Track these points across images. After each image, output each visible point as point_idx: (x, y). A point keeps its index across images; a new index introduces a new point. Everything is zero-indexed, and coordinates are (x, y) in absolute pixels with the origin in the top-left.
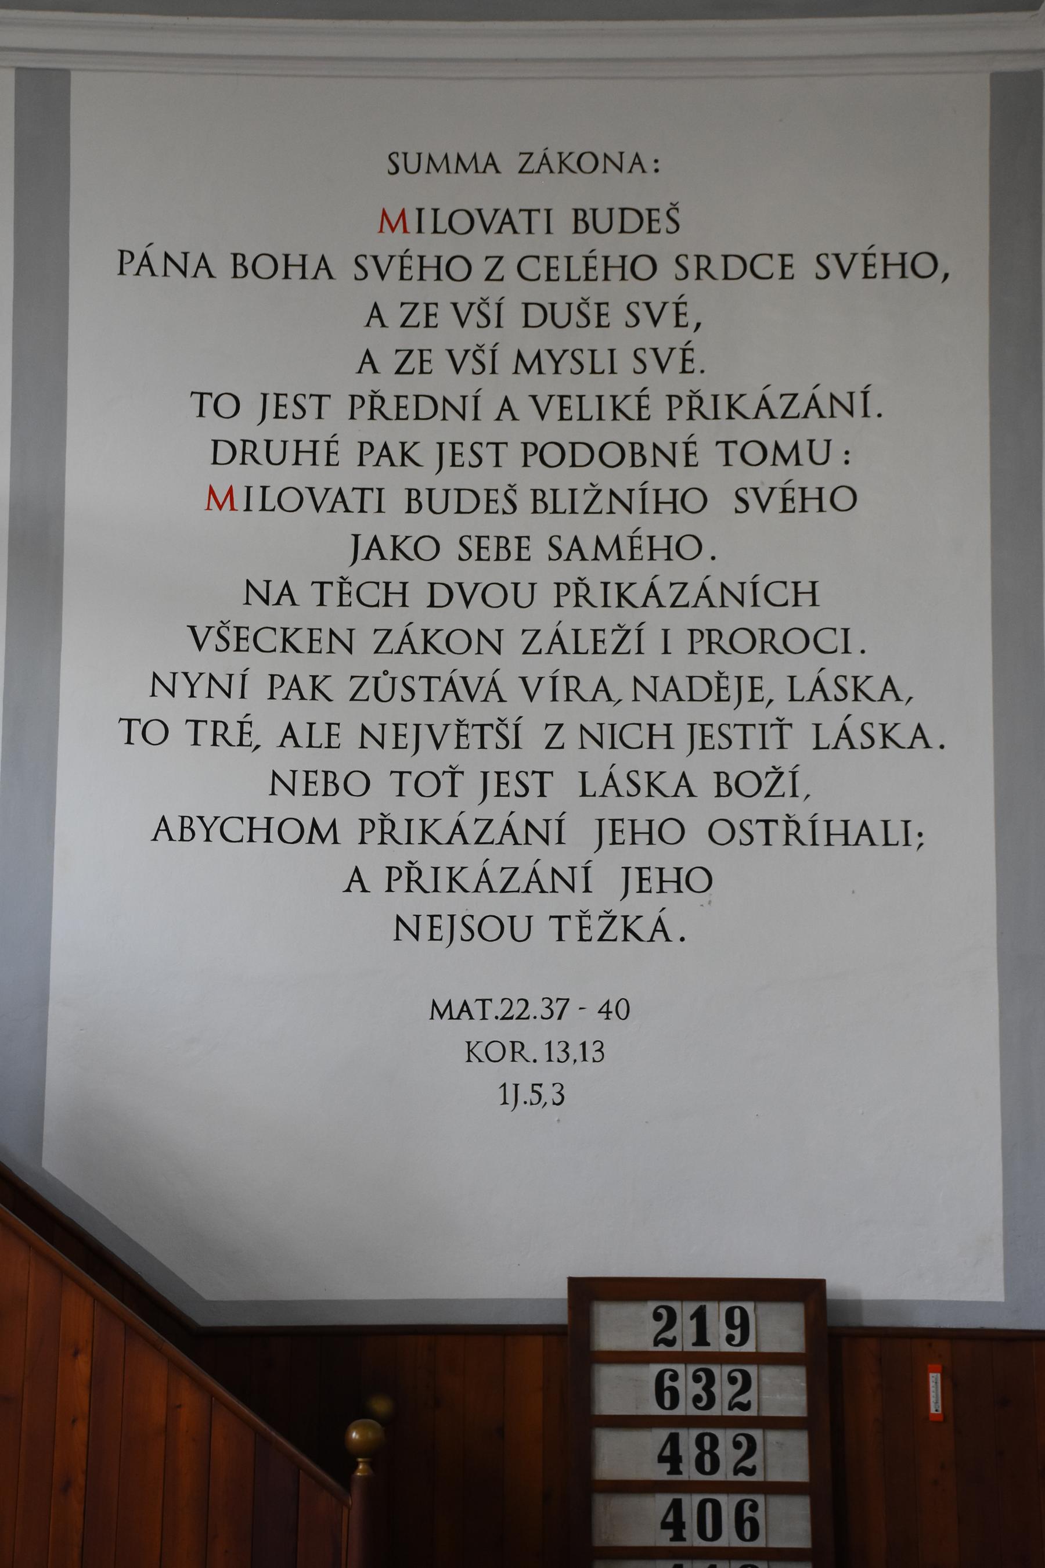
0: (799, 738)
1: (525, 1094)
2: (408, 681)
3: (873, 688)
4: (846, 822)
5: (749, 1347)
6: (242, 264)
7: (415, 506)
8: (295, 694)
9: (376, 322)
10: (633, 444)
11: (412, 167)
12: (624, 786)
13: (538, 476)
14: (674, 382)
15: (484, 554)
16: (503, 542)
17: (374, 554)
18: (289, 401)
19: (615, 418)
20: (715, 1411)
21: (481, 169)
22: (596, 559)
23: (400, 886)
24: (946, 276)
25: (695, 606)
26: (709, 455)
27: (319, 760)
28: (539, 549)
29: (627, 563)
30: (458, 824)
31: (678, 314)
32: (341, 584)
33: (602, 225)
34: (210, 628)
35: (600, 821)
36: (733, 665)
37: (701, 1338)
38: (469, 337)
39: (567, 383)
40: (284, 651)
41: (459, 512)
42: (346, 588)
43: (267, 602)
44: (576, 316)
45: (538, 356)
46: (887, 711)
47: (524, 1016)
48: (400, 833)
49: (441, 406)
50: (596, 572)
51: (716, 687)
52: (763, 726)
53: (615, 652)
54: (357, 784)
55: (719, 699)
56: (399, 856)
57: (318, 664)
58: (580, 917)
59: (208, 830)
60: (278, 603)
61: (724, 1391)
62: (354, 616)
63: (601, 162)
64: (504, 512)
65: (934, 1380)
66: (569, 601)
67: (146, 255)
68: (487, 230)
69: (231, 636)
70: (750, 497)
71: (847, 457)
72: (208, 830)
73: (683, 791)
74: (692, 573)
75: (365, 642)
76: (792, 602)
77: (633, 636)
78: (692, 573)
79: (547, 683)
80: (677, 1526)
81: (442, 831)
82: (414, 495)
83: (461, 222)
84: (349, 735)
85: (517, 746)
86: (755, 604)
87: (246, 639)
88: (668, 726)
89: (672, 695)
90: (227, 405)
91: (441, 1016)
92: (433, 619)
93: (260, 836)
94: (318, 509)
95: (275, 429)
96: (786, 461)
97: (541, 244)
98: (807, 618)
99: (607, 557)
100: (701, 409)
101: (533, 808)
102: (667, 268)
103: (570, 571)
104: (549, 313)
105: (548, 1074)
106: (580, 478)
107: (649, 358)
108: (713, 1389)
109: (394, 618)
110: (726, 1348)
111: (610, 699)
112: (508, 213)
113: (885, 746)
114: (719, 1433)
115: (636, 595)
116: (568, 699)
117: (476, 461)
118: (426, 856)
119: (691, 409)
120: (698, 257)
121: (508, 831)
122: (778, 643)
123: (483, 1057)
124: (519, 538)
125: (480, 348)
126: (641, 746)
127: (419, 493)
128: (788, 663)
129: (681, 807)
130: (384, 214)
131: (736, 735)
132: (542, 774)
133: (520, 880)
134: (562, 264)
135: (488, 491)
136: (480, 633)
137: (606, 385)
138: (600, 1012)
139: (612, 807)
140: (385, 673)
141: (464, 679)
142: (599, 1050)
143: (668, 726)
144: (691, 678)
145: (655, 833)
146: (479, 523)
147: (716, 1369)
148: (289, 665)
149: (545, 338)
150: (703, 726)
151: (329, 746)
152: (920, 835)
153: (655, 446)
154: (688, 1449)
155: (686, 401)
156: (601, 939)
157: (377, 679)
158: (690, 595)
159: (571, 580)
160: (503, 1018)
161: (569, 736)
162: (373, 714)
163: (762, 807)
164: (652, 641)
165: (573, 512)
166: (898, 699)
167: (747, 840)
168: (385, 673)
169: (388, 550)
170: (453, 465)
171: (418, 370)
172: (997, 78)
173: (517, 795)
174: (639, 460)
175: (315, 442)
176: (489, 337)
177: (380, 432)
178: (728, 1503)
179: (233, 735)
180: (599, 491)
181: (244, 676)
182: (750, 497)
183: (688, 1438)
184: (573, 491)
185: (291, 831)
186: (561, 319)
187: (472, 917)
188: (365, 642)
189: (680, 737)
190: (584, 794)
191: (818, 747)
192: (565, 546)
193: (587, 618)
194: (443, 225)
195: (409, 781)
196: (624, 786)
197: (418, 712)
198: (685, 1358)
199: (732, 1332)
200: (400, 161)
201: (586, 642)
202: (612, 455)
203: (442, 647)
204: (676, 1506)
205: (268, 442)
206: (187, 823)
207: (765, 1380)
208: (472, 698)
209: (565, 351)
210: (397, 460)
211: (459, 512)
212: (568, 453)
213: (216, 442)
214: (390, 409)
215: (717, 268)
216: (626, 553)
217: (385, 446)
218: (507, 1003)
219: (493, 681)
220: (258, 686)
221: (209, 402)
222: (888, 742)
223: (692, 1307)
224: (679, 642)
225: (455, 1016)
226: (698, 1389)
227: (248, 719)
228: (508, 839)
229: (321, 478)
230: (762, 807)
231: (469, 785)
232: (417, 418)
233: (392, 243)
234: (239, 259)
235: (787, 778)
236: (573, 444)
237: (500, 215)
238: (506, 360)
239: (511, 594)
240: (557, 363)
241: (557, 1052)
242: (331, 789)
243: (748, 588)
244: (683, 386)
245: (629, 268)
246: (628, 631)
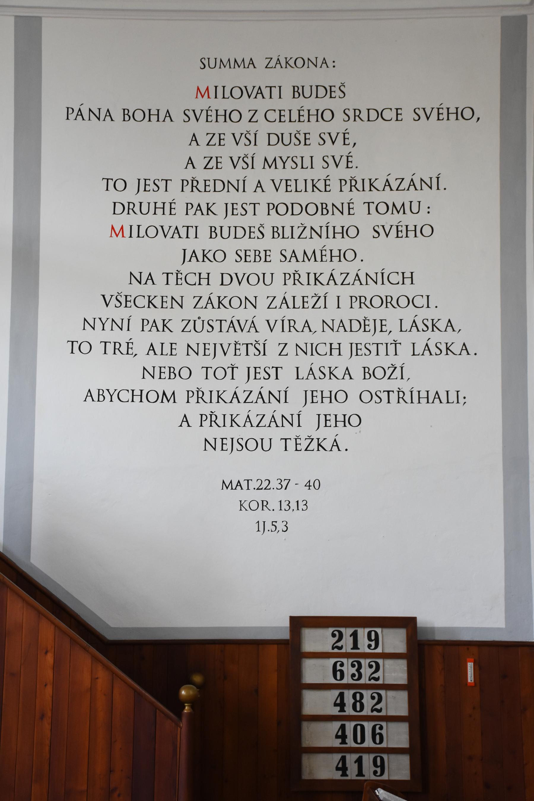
0: (405, 350)
1: (269, 526)
2: (210, 322)
3: (442, 325)
4: (428, 392)
5: (379, 650)
6: (127, 114)
7: (214, 235)
8: (154, 329)
9: (194, 143)
10: (322, 204)
11: (212, 65)
12: (318, 374)
13: (275, 220)
14: (343, 172)
15: (248, 259)
16: (257, 253)
17: (194, 259)
18: (151, 183)
19: (313, 191)
20: (362, 681)
21: (246, 66)
22: (304, 261)
23: (206, 423)
24: (478, 119)
25: (353, 284)
26: (360, 209)
27: (166, 361)
28: (275, 256)
29: (319, 263)
30: (235, 393)
31: (344, 139)
32: (177, 274)
33: (307, 94)
34: (112, 296)
35: (306, 391)
36: (372, 314)
37: (355, 646)
39: (289, 173)
40: (149, 307)
41: (235, 238)
42: (180, 276)
43: (140, 283)
44: (294, 140)
45: (275, 160)
46: (448, 337)
47: (268, 488)
48: (207, 398)
49: (227, 185)
50: (304, 268)
51: (363, 325)
52: (387, 344)
53: (313, 307)
54: (185, 373)
55: (365, 331)
56: (206, 409)
57: (166, 314)
58: (296, 439)
59: (111, 396)
60: (146, 283)
61: (366, 672)
62: (183, 290)
64: (258, 238)
65: (470, 666)
66: (290, 282)
67: (80, 110)
68: (249, 97)
69: (123, 300)
70: (381, 230)
71: (429, 210)
72: (111, 396)
73: (347, 376)
74: (352, 268)
75: (189, 303)
76: (401, 282)
77: (322, 300)
78: (352, 268)
79: (279, 323)
80: (343, 737)
81: (227, 397)
82: (213, 229)
83: (237, 93)
84: (181, 349)
85: (264, 354)
86: (383, 284)
87: (130, 301)
88: (339, 344)
89: (342, 329)
90: (120, 185)
91: (227, 488)
92: (223, 291)
93: (137, 399)
94: (165, 236)
95: (144, 197)
96: (398, 212)
97: (276, 103)
98: (409, 290)
99: (309, 260)
100: (356, 186)
101: (272, 385)
102: (339, 116)
103: (291, 267)
104: (280, 138)
105: (280, 516)
106: (296, 221)
107: (330, 161)
108: (361, 671)
109: (203, 291)
110: (368, 650)
111: (310, 331)
112: (260, 88)
113: (447, 354)
114: (364, 692)
115: (324, 279)
116: (290, 331)
117: (244, 213)
118: (220, 409)
119: (351, 186)
120: (355, 110)
121: (260, 396)
122: (394, 303)
123: (248, 508)
124: (266, 251)
125: (246, 156)
126: (326, 354)
127: (215, 229)
128: (399, 313)
129: (346, 384)
130: (198, 89)
131: (373, 348)
132: (277, 368)
133: (266, 421)
134: (287, 114)
135: (250, 227)
136: (246, 298)
137: (309, 174)
138: (305, 486)
139: (311, 384)
140: (199, 318)
141: (238, 321)
142: (305, 505)
143: (339, 344)
144: (351, 320)
145: (333, 397)
146: (246, 244)
147: (362, 661)
148: (151, 314)
149: (279, 151)
150: (357, 344)
151: (171, 355)
152: (465, 398)
153: (333, 205)
154: (349, 700)
155: (349, 182)
156: (306, 450)
157: (195, 321)
158: (350, 279)
159: (291, 272)
160: (258, 489)
161: (291, 349)
162: (193, 339)
163: (386, 384)
164: (332, 302)
165: (292, 237)
166: (454, 331)
167: (379, 400)
168: (199, 318)
169: (200, 257)
170: (233, 214)
171: (215, 167)
172: (504, 19)
173: (264, 378)
174: (325, 212)
175: (164, 203)
176: (250, 150)
177: (196, 198)
178: (368, 726)
179: (124, 349)
180: (305, 227)
181: (129, 320)
182: (381, 230)
183: (348, 695)
184: (292, 227)
185: (152, 397)
186: (286, 141)
187: (242, 439)
188: (189, 303)
189: (346, 349)
190: (298, 378)
191: (414, 355)
192: (288, 255)
193: (299, 291)
194: (227, 94)
195: (211, 372)
196: (318, 374)
197: (215, 337)
198: (347, 655)
199: (370, 643)
200: (206, 62)
201: (299, 303)
202: (312, 209)
203: (227, 305)
204: (343, 727)
205: (141, 203)
206: (101, 392)
207: (387, 666)
208: (242, 331)
209: (288, 157)
210: (205, 212)
211: (235, 238)
212: (290, 208)
213: (115, 203)
214: (201, 187)
215: (364, 116)
216: (318, 258)
217: (199, 205)
218: (259, 482)
219: (253, 322)
220: (136, 325)
221: (111, 183)
222: (449, 352)
223: (351, 631)
224: (345, 302)
225: (234, 488)
226: (353, 670)
227: (131, 341)
228: (260, 400)
229: (167, 221)
230: (386, 384)
231: (241, 374)
232: (215, 191)
233: (202, 104)
234: (126, 112)
235: (398, 370)
236: (292, 204)
237: (256, 89)
238: (259, 162)
239: (262, 279)
240: (284, 163)
241: (284, 506)
242: (172, 375)
243: (380, 275)
244: (347, 174)
245: (320, 115)
246: (320, 297)
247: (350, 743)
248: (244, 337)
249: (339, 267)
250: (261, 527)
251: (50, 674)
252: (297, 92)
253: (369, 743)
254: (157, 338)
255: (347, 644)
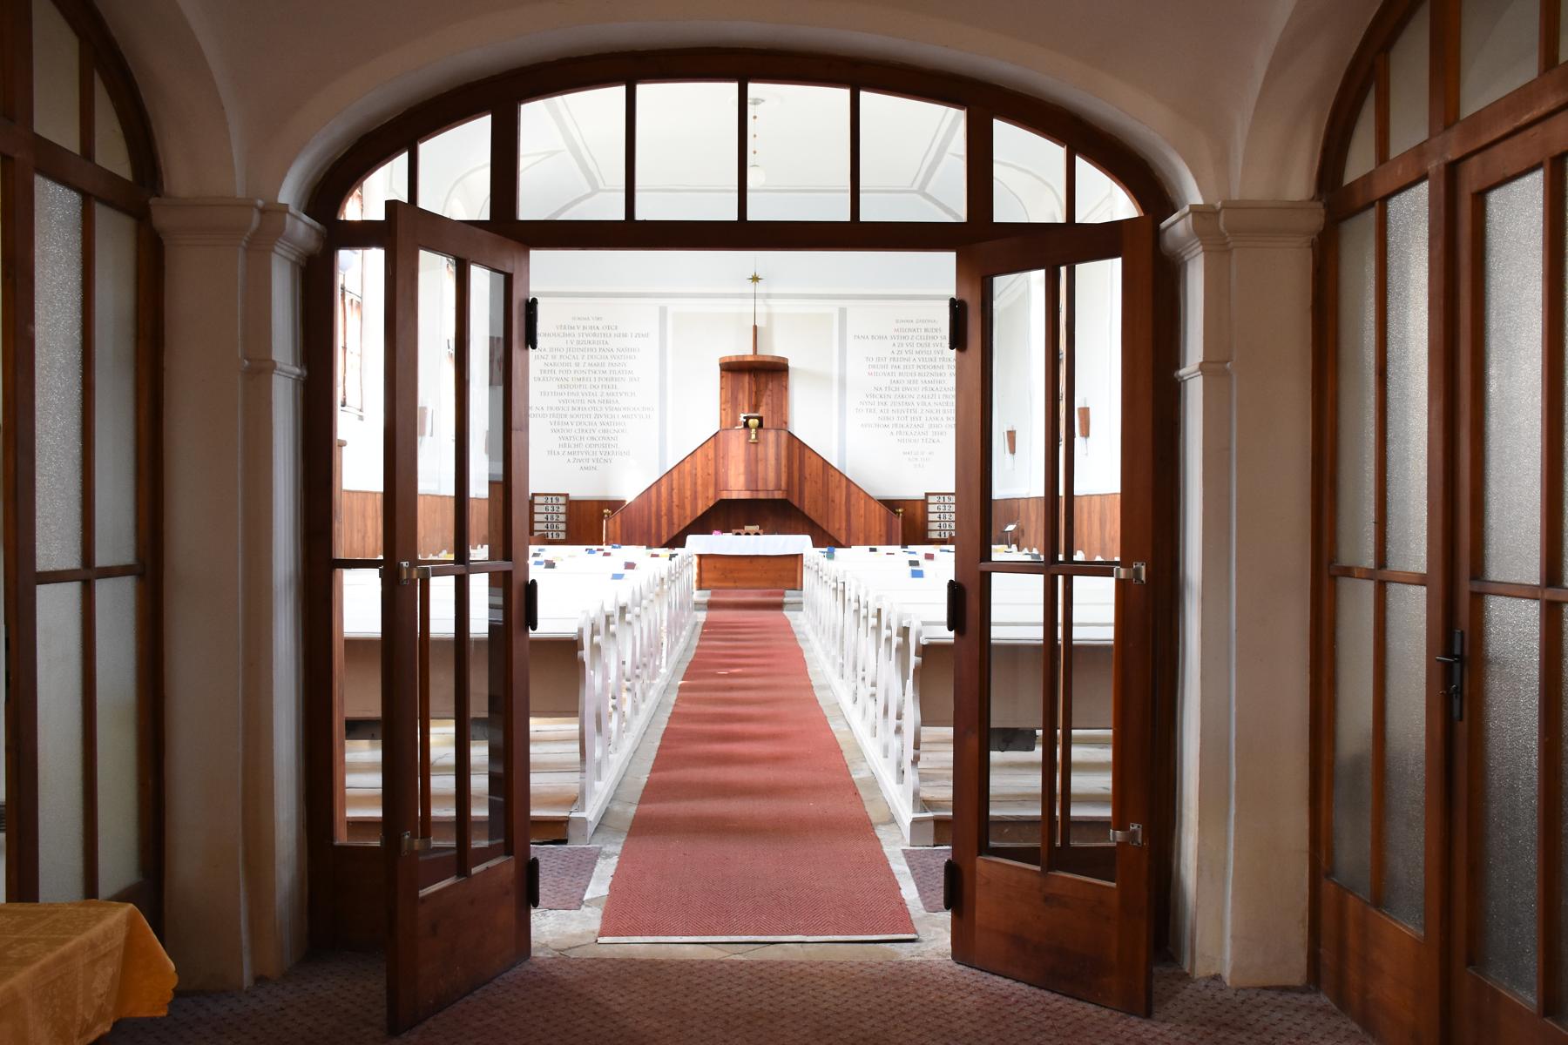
14: (940, 356)
38: (909, 348)
56: (898, 429)
61: (947, 508)
63: (929, 321)
103: (924, 386)
104: (921, 345)
106: (926, 371)
145: (937, 426)
162: (895, 408)
176: (912, 348)
193: (927, 393)
212: (924, 367)
220: (876, 404)
233: (896, 334)
238: (914, 352)
247: (942, 528)
248: (910, 407)
249: (939, 386)
250: (916, 465)
251: (863, 506)
252: (926, 330)
253: (948, 528)
254: (883, 407)
255: (942, 501)
